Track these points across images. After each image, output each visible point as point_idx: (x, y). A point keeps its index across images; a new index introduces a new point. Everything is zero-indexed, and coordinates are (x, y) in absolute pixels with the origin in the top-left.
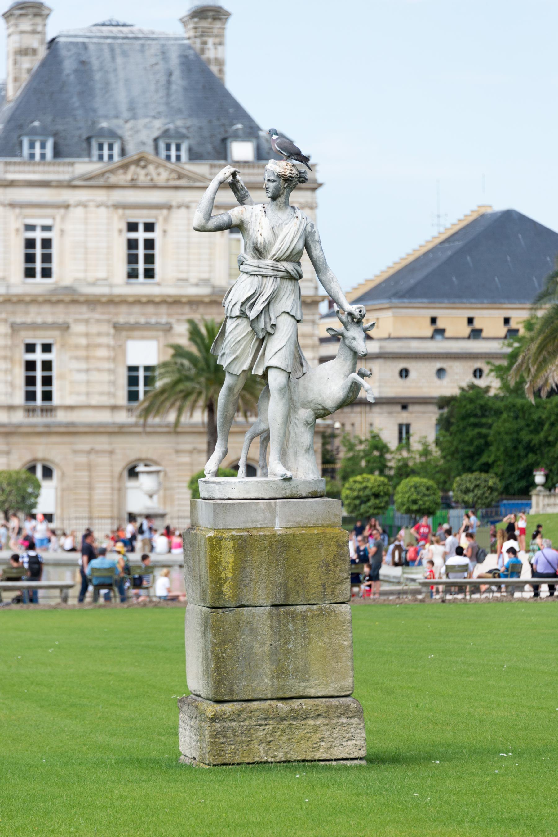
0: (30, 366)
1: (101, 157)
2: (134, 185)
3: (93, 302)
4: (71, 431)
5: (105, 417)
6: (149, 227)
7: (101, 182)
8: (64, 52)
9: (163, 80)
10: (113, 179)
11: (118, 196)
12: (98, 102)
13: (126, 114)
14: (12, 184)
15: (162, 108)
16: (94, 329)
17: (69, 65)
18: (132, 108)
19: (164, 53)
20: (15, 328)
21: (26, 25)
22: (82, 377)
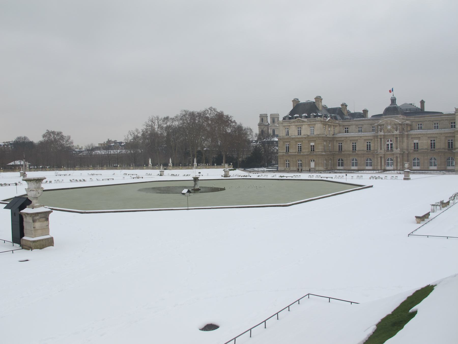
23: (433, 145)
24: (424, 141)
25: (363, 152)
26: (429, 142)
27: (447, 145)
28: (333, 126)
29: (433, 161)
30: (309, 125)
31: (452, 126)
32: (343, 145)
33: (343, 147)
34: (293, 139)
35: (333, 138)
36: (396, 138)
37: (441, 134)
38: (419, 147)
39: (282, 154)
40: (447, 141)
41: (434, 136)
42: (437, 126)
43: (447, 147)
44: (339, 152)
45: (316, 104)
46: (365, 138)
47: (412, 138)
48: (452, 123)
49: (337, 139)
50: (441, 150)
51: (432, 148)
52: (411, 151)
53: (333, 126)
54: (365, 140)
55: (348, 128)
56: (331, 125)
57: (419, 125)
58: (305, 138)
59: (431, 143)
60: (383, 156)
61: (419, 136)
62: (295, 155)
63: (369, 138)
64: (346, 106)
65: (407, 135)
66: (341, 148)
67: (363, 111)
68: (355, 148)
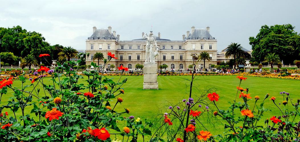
3: (198, 51)
6: (203, 45)
10: (200, 41)
11: (200, 42)
17: (197, 32)
19: (204, 31)
23: (173, 57)
25: (135, 61)
27: (180, 57)
29: (173, 66)
30: (107, 43)
31: (180, 48)
32: (123, 56)
33: (123, 57)
35: (117, 52)
38: (166, 59)
43: (180, 59)
44: (120, 60)
45: (109, 31)
46: (137, 52)
47: (162, 53)
48: (180, 46)
49: (120, 53)
50: (177, 60)
51: (172, 59)
52: (162, 61)
54: (136, 54)
55: (123, 46)
58: (105, 51)
61: (166, 52)
63: (139, 52)
65: (160, 52)
66: (121, 58)
67: (117, 35)
68: (131, 58)
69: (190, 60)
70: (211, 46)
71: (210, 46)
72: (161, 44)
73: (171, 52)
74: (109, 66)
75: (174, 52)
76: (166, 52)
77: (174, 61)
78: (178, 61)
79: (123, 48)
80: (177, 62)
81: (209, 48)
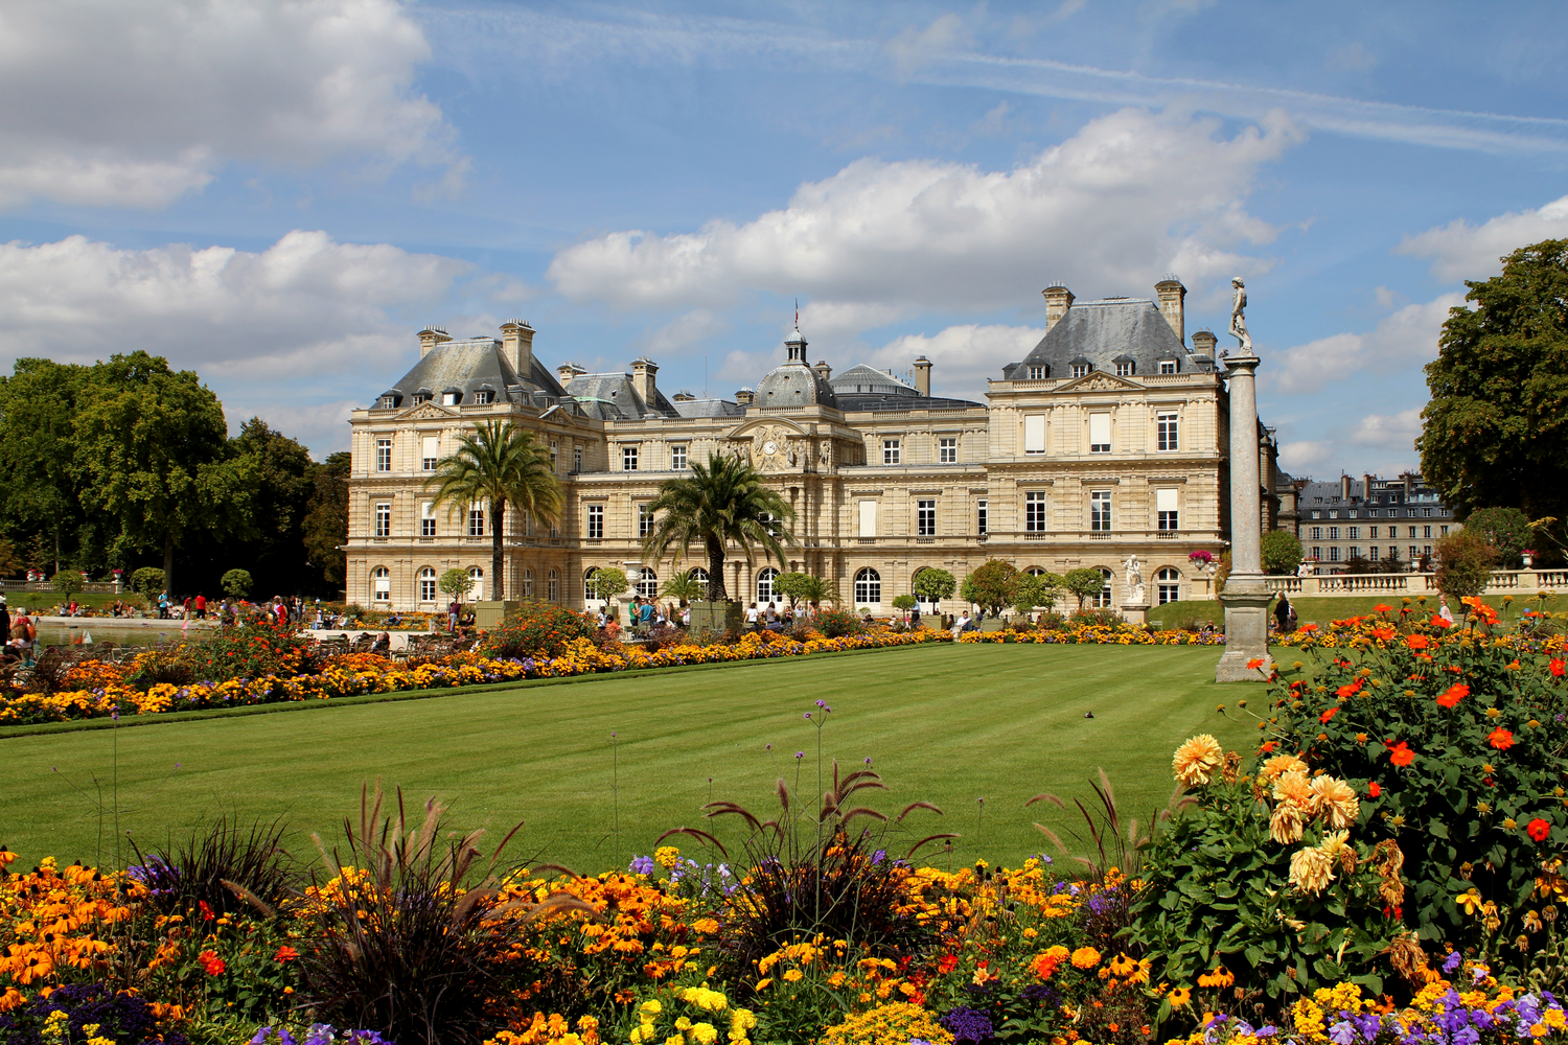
0: (1030, 507)
1: (1076, 375)
2: (1093, 393)
3: (1067, 466)
4: (1053, 549)
5: (1075, 539)
7: (1073, 390)
8: (1072, 315)
9: (1130, 327)
10: (1081, 388)
12: (1086, 345)
13: (1101, 349)
14: (1015, 395)
15: (1126, 344)
16: (1068, 483)
18: (1106, 346)
20: (1019, 484)
21: (1053, 301)
22: (1062, 514)
24: (897, 507)
26: (915, 509)
27: (975, 520)
28: (574, 437)
34: (404, 482)
36: (794, 490)
37: (954, 477)
39: (362, 543)
40: (975, 508)
41: (930, 486)
42: (952, 452)
47: (854, 494)
53: (574, 437)
56: (562, 436)
57: (887, 444)
59: (922, 514)
60: (743, 559)
62: (411, 551)
64: (652, 370)
69: (1010, 540)
70: (1167, 422)
71: (1162, 427)
72: (869, 429)
73: (914, 486)
74: (429, 578)
75: (937, 485)
76: (879, 486)
77: (938, 544)
78: (963, 543)
79: (634, 461)
80: (956, 551)
81: (1154, 440)
